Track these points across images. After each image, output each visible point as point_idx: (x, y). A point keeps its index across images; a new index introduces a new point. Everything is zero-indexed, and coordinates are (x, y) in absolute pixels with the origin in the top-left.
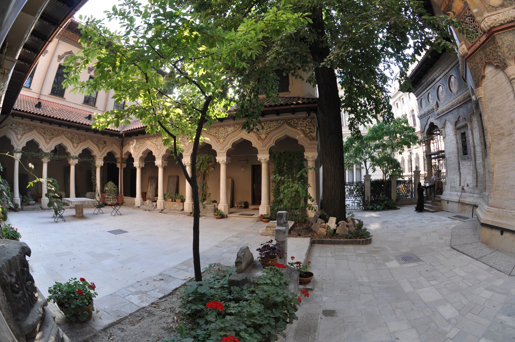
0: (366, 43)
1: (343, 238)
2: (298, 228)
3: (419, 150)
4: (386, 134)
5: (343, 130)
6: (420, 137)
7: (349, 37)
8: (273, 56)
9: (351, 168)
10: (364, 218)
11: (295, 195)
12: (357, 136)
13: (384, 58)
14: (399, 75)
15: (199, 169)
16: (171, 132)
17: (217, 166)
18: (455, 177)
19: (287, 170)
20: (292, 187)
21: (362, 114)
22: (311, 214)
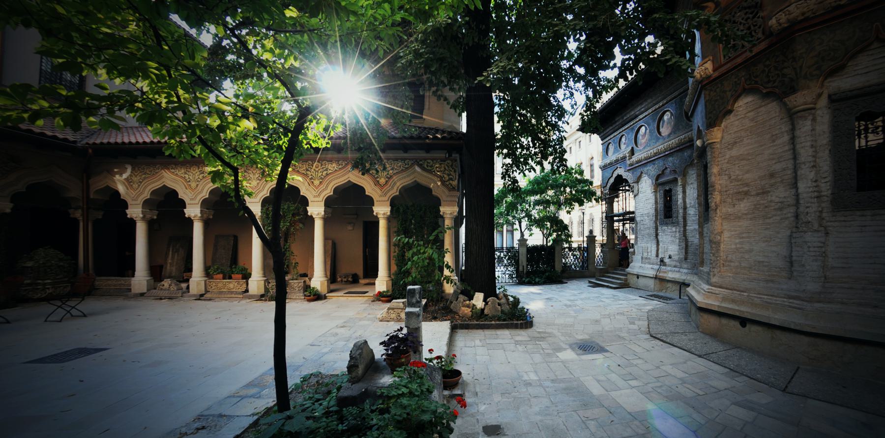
3: (595, 211)
6: (599, 193)
8: (410, 57)
9: (499, 229)
10: (520, 294)
12: (513, 188)
18: (649, 245)
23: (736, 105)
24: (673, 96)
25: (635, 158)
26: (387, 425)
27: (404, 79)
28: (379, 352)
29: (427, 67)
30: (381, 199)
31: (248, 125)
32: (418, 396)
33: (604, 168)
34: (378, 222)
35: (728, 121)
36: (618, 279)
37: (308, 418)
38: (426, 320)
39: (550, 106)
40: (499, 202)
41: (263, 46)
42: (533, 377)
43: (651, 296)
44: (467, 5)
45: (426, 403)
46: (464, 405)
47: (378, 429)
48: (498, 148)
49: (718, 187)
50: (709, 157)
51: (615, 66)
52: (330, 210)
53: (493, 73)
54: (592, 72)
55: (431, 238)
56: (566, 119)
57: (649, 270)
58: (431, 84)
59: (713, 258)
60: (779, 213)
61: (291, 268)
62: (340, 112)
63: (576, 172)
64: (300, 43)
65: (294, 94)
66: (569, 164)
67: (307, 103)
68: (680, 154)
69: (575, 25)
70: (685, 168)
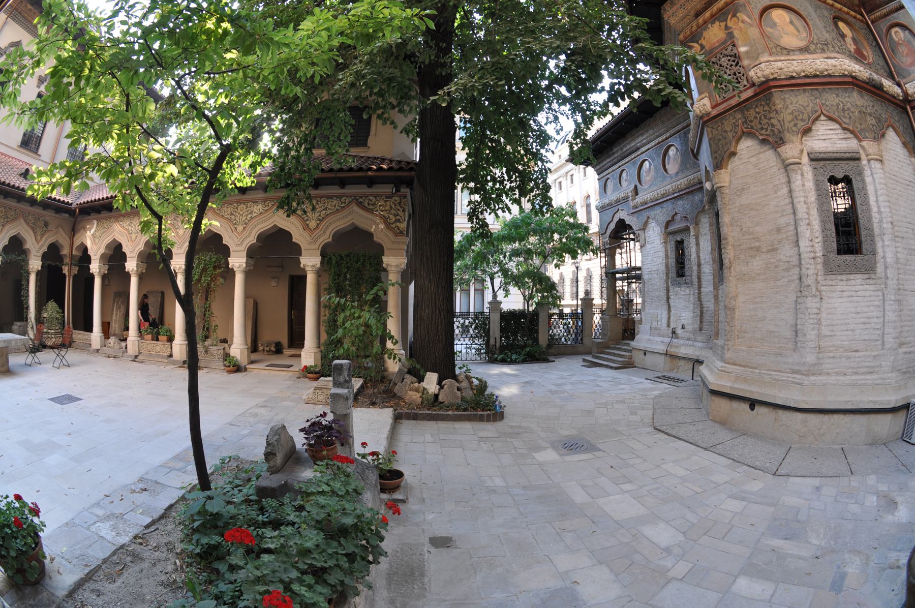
0: (522, 73)
2: (370, 391)
4: (535, 234)
5: (456, 220)
6: (596, 242)
7: (495, 59)
9: (465, 287)
11: (365, 332)
13: (550, 104)
14: (571, 134)
15: (199, 280)
16: (155, 209)
17: (229, 274)
18: (659, 311)
19: (351, 286)
20: (359, 317)
21: (494, 196)
22: (393, 366)
23: (738, 148)
24: (676, 129)
25: (639, 200)
30: (309, 247)
33: (601, 209)
34: (306, 277)
35: (734, 164)
36: (620, 356)
43: (660, 377)
48: (462, 180)
49: (730, 240)
50: (719, 203)
52: (252, 262)
57: (658, 344)
59: (727, 328)
60: (787, 274)
61: (211, 330)
66: (555, 204)
68: (690, 197)
70: (697, 217)
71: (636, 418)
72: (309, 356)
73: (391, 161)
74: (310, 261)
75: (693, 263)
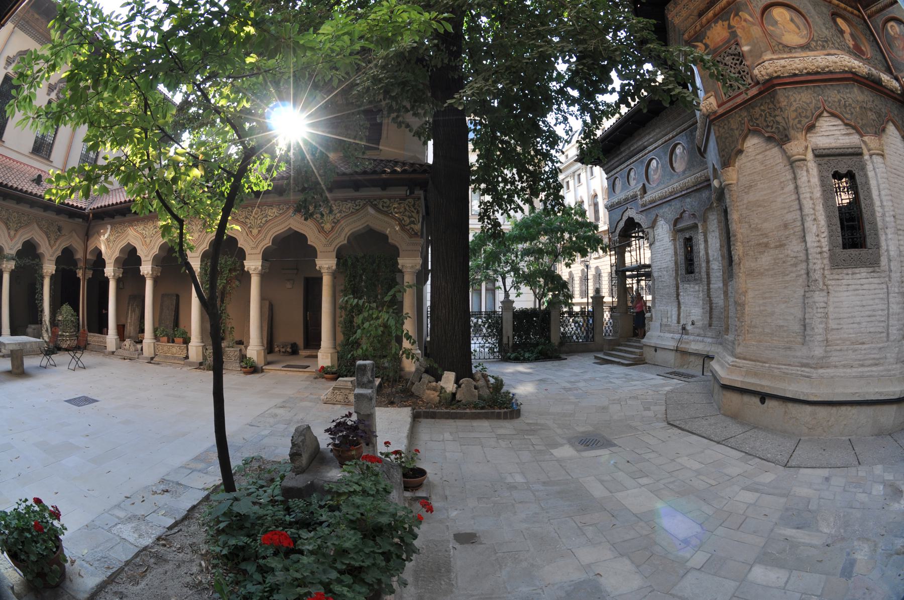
1: (470, 408)
3: (602, 263)
6: (606, 240)
11: (383, 332)
17: (247, 276)
18: (669, 308)
20: (377, 318)
23: (745, 146)
25: (647, 198)
26: (339, 523)
27: (359, 106)
28: (325, 441)
29: (387, 92)
31: (197, 173)
32: (373, 496)
33: (610, 208)
34: (321, 279)
35: (741, 162)
36: (631, 353)
37: (254, 503)
38: (380, 404)
39: (540, 132)
40: (476, 252)
41: (221, 94)
42: (519, 479)
43: (671, 373)
44: (436, 30)
45: (383, 504)
46: (430, 509)
47: (328, 526)
48: (473, 182)
49: (739, 236)
50: (728, 200)
51: (613, 90)
52: (267, 264)
53: (465, 96)
54: (588, 94)
55: (387, 299)
56: (560, 147)
58: (390, 109)
59: (738, 323)
61: (227, 333)
62: (285, 149)
63: (576, 213)
64: (254, 85)
65: (241, 134)
67: (252, 143)
69: (563, 47)
70: (705, 213)
71: (650, 414)
72: (325, 357)
73: (404, 164)
74: (326, 263)
75: (702, 259)
